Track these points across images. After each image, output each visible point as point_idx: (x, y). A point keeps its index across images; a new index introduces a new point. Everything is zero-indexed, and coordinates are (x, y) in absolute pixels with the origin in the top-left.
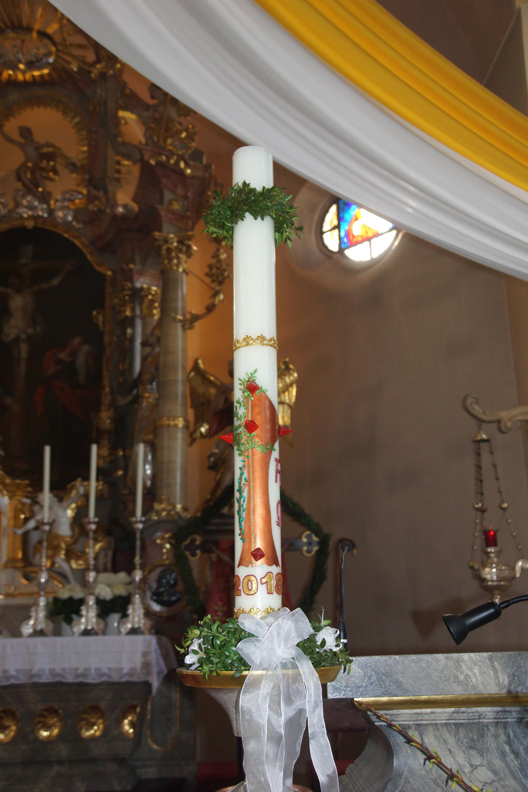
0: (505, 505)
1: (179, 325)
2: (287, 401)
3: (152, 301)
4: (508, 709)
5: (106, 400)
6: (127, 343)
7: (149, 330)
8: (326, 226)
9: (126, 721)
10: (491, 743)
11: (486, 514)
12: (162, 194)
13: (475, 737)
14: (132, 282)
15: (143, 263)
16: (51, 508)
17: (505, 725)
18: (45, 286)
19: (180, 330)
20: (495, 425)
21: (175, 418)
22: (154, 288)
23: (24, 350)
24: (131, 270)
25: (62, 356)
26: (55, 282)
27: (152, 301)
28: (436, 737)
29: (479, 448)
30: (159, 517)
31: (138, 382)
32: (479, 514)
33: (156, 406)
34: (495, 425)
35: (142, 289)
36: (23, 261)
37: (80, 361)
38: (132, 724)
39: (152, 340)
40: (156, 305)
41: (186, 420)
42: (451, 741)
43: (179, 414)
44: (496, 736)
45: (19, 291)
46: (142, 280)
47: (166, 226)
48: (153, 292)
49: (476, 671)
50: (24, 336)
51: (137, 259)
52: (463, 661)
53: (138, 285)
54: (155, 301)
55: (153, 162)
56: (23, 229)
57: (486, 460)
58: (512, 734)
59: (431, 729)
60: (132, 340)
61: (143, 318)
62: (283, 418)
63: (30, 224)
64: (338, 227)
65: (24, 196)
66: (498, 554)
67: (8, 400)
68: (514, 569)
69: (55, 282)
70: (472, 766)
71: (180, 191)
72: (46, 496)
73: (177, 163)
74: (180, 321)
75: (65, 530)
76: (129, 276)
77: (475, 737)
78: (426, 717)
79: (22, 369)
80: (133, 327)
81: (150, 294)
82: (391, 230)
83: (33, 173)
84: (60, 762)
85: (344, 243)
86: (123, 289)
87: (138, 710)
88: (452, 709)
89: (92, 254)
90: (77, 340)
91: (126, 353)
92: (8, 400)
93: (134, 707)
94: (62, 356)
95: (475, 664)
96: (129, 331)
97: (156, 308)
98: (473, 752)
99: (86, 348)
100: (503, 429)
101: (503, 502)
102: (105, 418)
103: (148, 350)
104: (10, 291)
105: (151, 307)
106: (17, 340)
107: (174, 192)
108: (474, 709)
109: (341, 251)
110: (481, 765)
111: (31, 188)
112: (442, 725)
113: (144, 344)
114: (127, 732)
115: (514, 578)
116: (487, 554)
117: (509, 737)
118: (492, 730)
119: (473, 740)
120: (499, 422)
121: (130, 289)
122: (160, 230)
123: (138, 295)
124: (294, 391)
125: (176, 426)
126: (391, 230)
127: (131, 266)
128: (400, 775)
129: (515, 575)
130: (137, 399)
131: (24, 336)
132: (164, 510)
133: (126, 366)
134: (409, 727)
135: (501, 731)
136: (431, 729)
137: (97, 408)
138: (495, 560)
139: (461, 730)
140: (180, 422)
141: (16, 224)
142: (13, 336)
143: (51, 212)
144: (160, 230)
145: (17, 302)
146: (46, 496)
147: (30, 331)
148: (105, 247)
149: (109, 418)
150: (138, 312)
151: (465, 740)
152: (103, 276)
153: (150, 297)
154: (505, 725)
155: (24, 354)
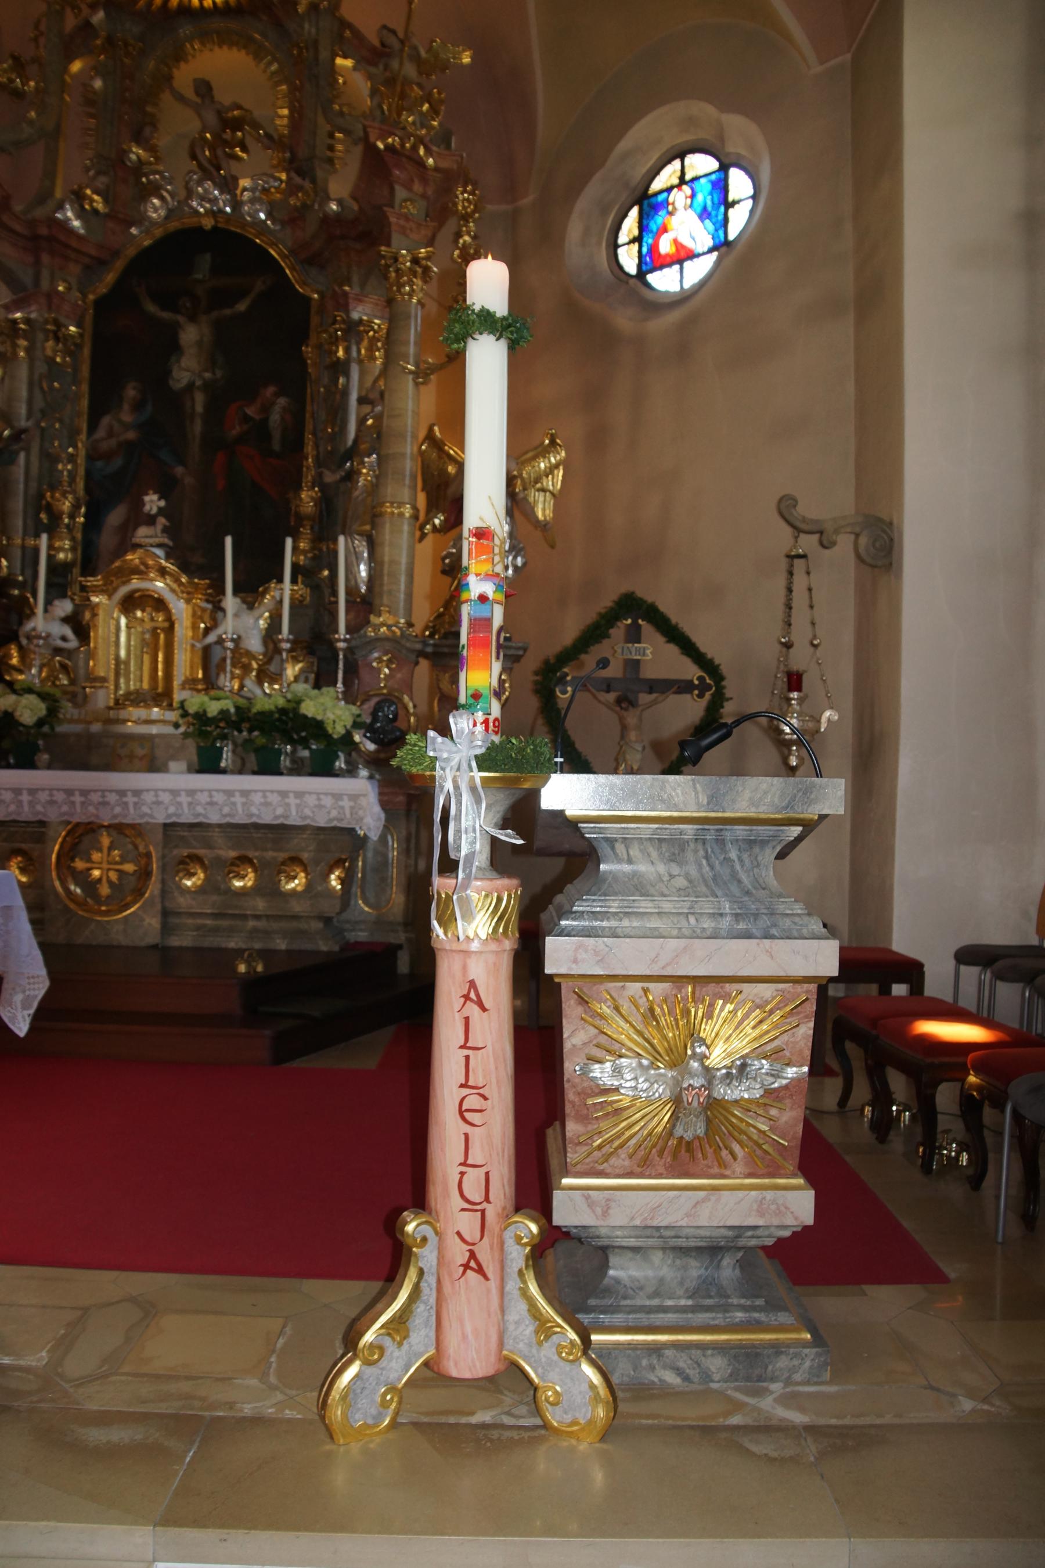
0: (815, 642)
1: (411, 377)
2: (551, 488)
3: (373, 341)
4: (707, 827)
5: (309, 477)
6: (338, 397)
7: (369, 383)
8: (623, 238)
9: (333, 877)
10: (690, 856)
11: (791, 650)
13: (677, 852)
14: (347, 312)
15: (363, 285)
16: (236, 615)
17: (704, 841)
18: (228, 312)
19: (411, 384)
20: (816, 536)
21: (401, 504)
22: (377, 321)
23: (199, 400)
24: (345, 294)
25: (250, 411)
26: (242, 307)
27: (373, 341)
28: (641, 850)
29: (792, 566)
30: (376, 634)
31: (352, 453)
32: (784, 649)
33: (374, 488)
34: (816, 536)
35: (361, 321)
36: (199, 276)
37: (275, 417)
38: (342, 881)
39: (374, 395)
40: (379, 344)
41: (415, 508)
42: (654, 854)
43: (407, 500)
44: (696, 851)
45: (193, 318)
46: (360, 308)
47: (396, 239)
48: (376, 327)
49: (679, 791)
50: (198, 383)
51: (355, 278)
52: (668, 781)
53: (355, 316)
54: (379, 340)
55: (381, 146)
56: (200, 229)
57: (800, 582)
58: (710, 850)
59: (636, 842)
60: (345, 393)
61: (360, 362)
62: (544, 510)
63: (208, 223)
64: (638, 240)
65: (200, 183)
66: (801, 701)
67: (179, 470)
68: (819, 721)
69: (242, 307)
70: (670, 875)
71: (417, 187)
72: (230, 602)
73: (415, 148)
74: (411, 372)
75: (255, 644)
77: (677, 852)
78: (632, 831)
79: (198, 427)
80: (347, 375)
81: (373, 329)
82: (710, 251)
83: (213, 149)
84: (257, 917)
85: (646, 264)
86: (335, 322)
87: (347, 864)
88: (656, 826)
89: (292, 269)
90: (271, 390)
91: (337, 412)
92: (179, 470)
93: (344, 861)
95: (679, 785)
96: (341, 380)
97: (378, 350)
98: (673, 865)
99: (282, 401)
100: (825, 542)
101: (815, 637)
102: (307, 499)
103: (367, 409)
104: (181, 319)
105: (371, 349)
106: (191, 386)
107: (409, 188)
108: (676, 826)
109: (641, 275)
110: (679, 875)
111: (211, 170)
112: (646, 839)
113: (361, 401)
114: (334, 888)
115: (818, 731)
116: (789, 700)
117: (707, 852)
118: (692, 845)
119: (674, 854)
120: (821, 533)
121: (344, 321)
122: (388, 244)
123: (354, 330)
124: (560, 473)
125: (401, 515)
126: (710, 251)
127: (347, 288)
128: (604, 881)
129: (820, 728)
130: (351, 476)
131: (198, 383)
132: (383, 624)
133: (336, 429)
134: (616, 840)
135: (700, 847)
136: (636, 842)
137: (298, 488)
138: (797, 708)
139: (663, 845)
140: (407, 511)
141: (190, 222)
142: (184, 382)
143: (236, 205)
144: (388, 244)
145: (190, 335)
146: (230, 602)
147: (207, 375)
148: (311, 259)
149: (312, 498)
150: (354, 354)
151: (667, 854)
152: (307, 300)
153: (371, 333)
154: (704, 841)
155: (199, 408)
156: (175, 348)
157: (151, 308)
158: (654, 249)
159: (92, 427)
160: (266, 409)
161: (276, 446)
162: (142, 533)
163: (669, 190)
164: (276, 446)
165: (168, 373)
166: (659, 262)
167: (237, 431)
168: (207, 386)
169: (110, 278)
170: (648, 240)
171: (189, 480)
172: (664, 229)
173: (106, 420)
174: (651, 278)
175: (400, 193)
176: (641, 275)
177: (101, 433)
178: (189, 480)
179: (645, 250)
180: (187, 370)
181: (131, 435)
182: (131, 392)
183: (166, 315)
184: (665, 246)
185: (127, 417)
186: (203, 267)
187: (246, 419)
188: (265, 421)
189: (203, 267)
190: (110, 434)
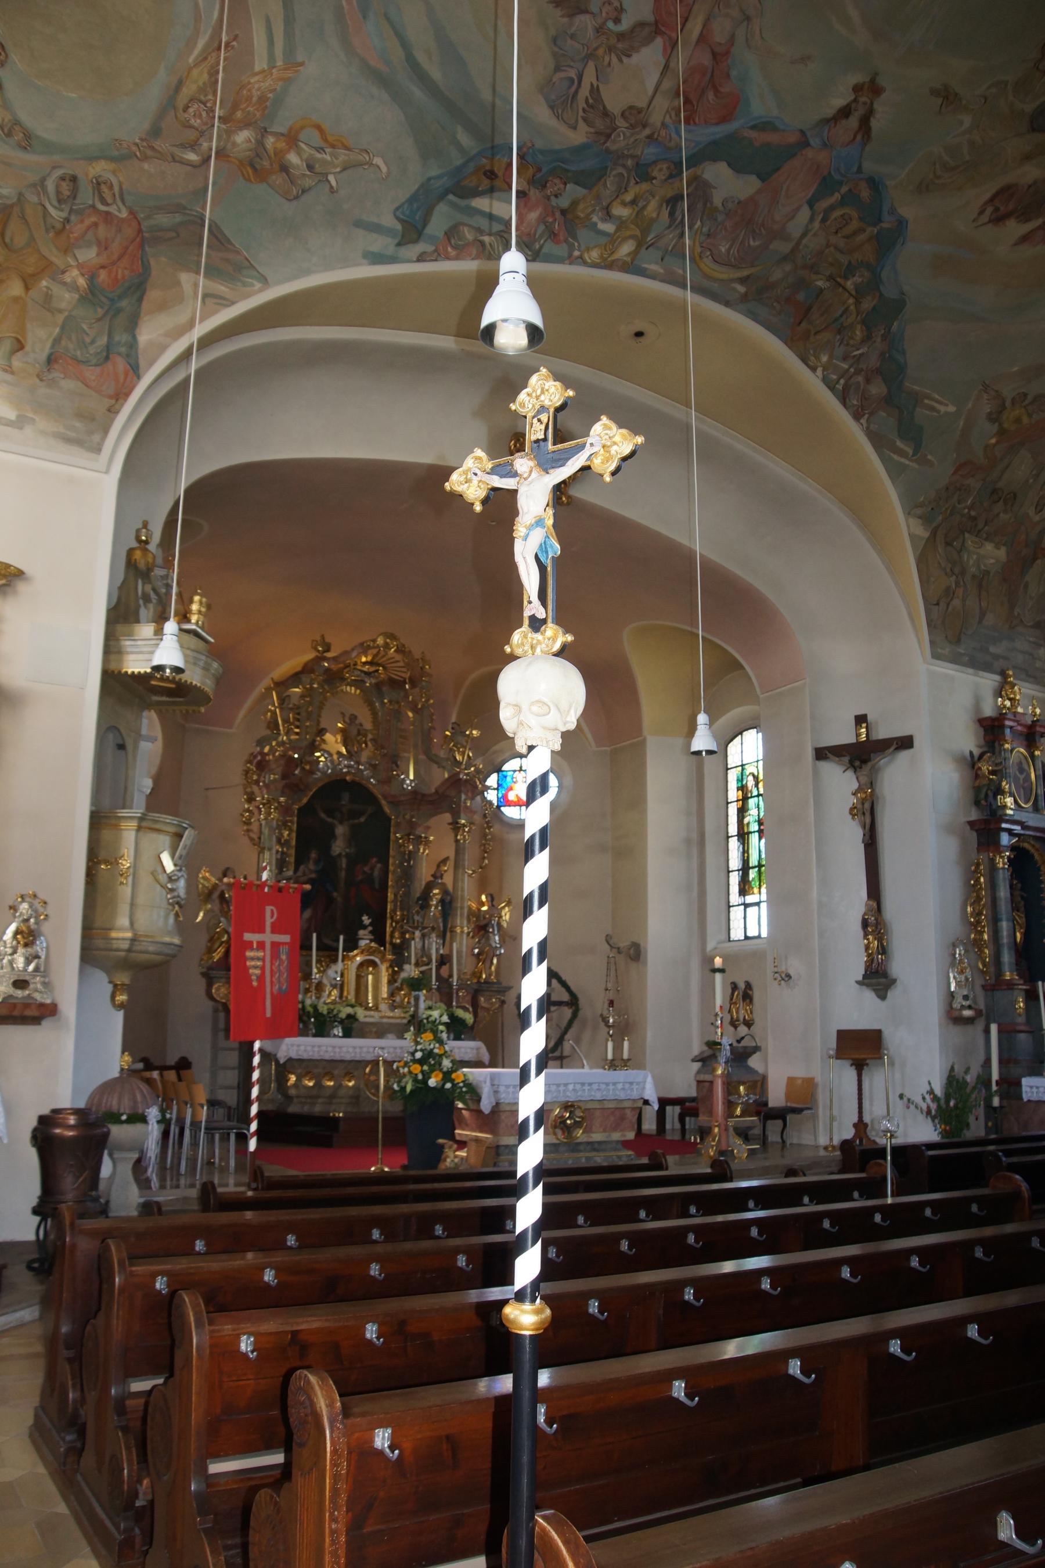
12: (459, 792)
18: (356, 821)
23: (344, 861)
25: (366, 869)
37: (376, 873)
45: (341, 822)
67: (335, 894)
69: (362, 820)
76: (412, 826)
79: (343, 874)
90: (375, 860)
92: (335, 894)
94: (366, 869)
99: (379, 865)
104: (336, 822)
106: (340, 855)
109: (498, 807)
123: (419, 840)
145: (340, 830)
155: (344, 866)
156: (333, 836)
157: (323, 815)
158: (505, 796)
159: (296, 871)
160: (372, 869)
161: (377, 886)
162: (361, 933)
163: (515, 771)
164: (377, 886)
165: (328, 848)
166: (509, 803)
167: (360, 877)
168: (347, 855)
169: (305, 800)
170: (502, 791)
171: (339, 899)
172: (511, 789)
173: (302, 868)
174: (502, 809)
175: (463, 797)
176: (498, 807)
177: (300, 873)
178: (339, 899)
179: (500, 795)
180: (338, 847)
181: (313, 876)
182: (313, 855)
183: (329, 820)
184: (512, 796)
185: (311, 866)
186: (346, 797)
187: (364, 873)
188: (372, 874)
189: (346, 797)
190: (304, 874)
